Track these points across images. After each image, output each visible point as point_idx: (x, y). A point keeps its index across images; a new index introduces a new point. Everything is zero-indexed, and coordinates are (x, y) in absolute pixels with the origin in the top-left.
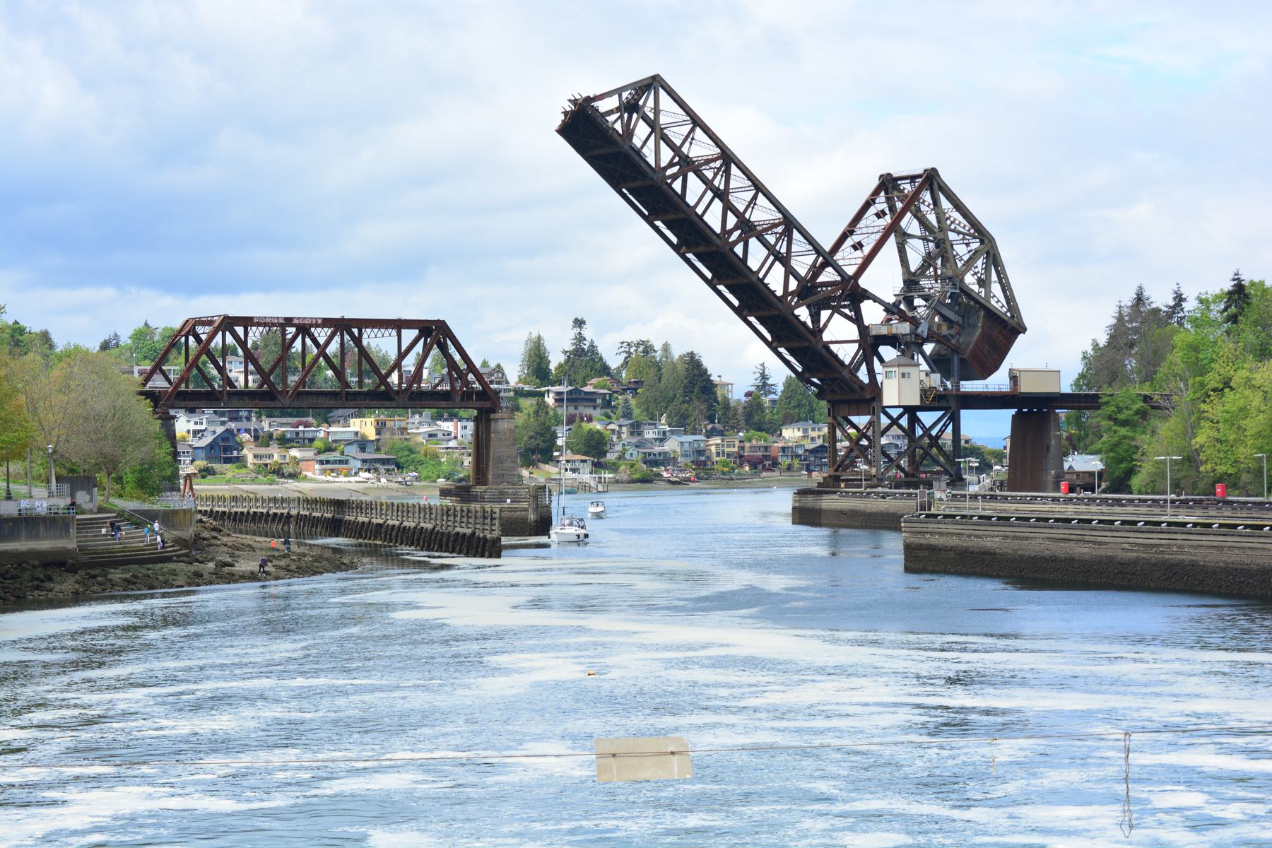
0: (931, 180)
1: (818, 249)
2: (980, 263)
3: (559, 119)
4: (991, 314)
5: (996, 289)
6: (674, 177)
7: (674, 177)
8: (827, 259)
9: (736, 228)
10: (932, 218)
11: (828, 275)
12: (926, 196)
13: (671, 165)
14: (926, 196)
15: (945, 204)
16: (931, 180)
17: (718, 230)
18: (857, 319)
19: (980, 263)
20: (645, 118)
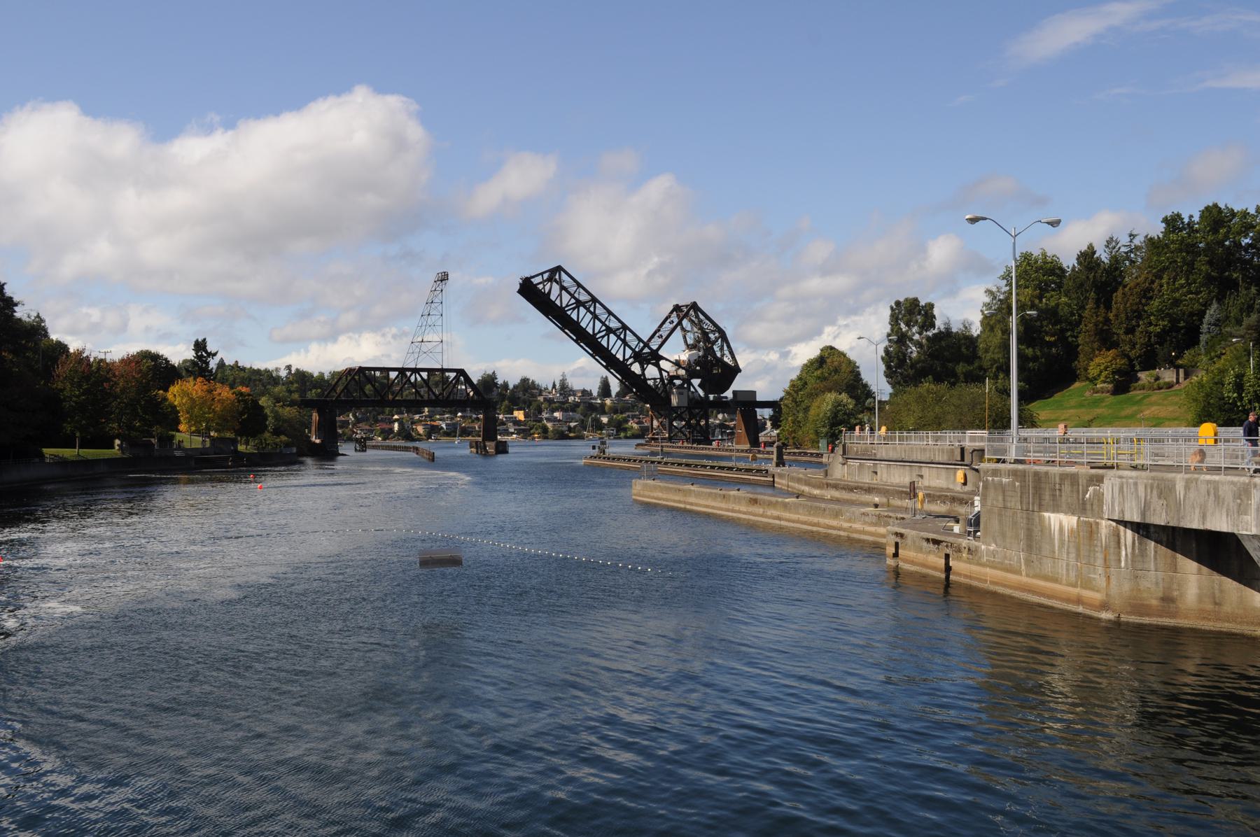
0: (694, 306)
1: (640, 340)
2: (720, 340)
3: (518, 287)
4: (726, 364)
5: (727, 352)
6: (603, 337)
7: (603, 337)
8: (646, 345)
9: (630, 357)
10: (696, 321)
11: (646, 350)
12: (692, 312)
13: (600, 332)
14: (692, 312)
15: (702, 317)
17: (591, 333)
18: (660, 370)
19: (720, 340)
20: (557, 282)
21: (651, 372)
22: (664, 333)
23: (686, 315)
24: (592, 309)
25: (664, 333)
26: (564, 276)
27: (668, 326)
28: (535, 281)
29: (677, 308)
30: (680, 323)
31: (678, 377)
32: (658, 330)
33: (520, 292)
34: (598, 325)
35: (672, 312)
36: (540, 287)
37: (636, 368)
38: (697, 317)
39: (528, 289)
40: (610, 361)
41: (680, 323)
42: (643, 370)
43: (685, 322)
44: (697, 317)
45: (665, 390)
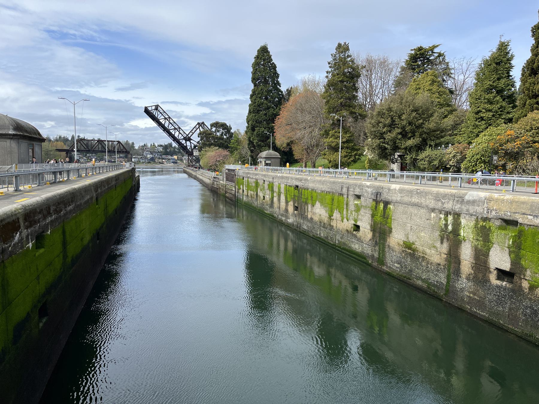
0: (203, 123)
8: (187, 135)
16: (203, 123)
21: (188, 143)
22: (193, 132)
23: (201, 125)
24: (169, 120)
25: (193, 132)
26: (159, 108)
27: (195, 129)
28: (150, 109)
29: (198, 124)
30: (199, 127)
31: (197, 146)
32: (192, 130)
33: (144, 112)
34: (170, 125)
35: (197, 125)
36: (151, 111)
37: (183, 142)
38: (203, 126)
39: (147, 111)
40: (175, 139)
41: (199, 127)
42: (186, 143)
43: (200, 127)
44: (203, 126)
45: (192, 150)
